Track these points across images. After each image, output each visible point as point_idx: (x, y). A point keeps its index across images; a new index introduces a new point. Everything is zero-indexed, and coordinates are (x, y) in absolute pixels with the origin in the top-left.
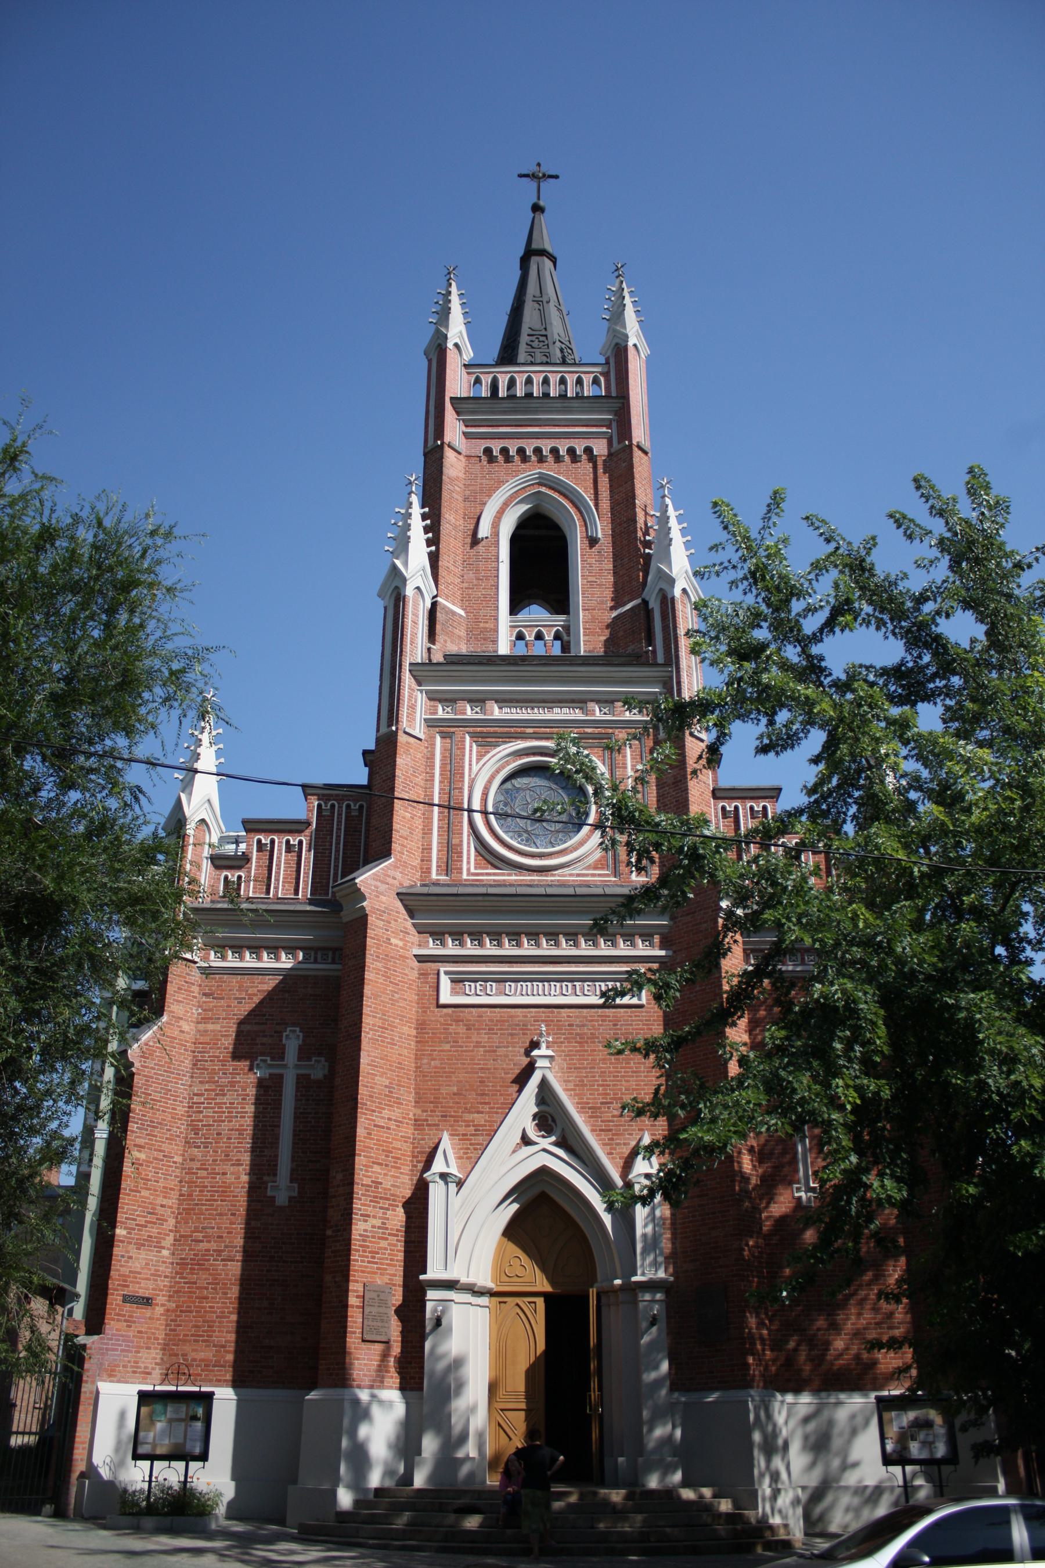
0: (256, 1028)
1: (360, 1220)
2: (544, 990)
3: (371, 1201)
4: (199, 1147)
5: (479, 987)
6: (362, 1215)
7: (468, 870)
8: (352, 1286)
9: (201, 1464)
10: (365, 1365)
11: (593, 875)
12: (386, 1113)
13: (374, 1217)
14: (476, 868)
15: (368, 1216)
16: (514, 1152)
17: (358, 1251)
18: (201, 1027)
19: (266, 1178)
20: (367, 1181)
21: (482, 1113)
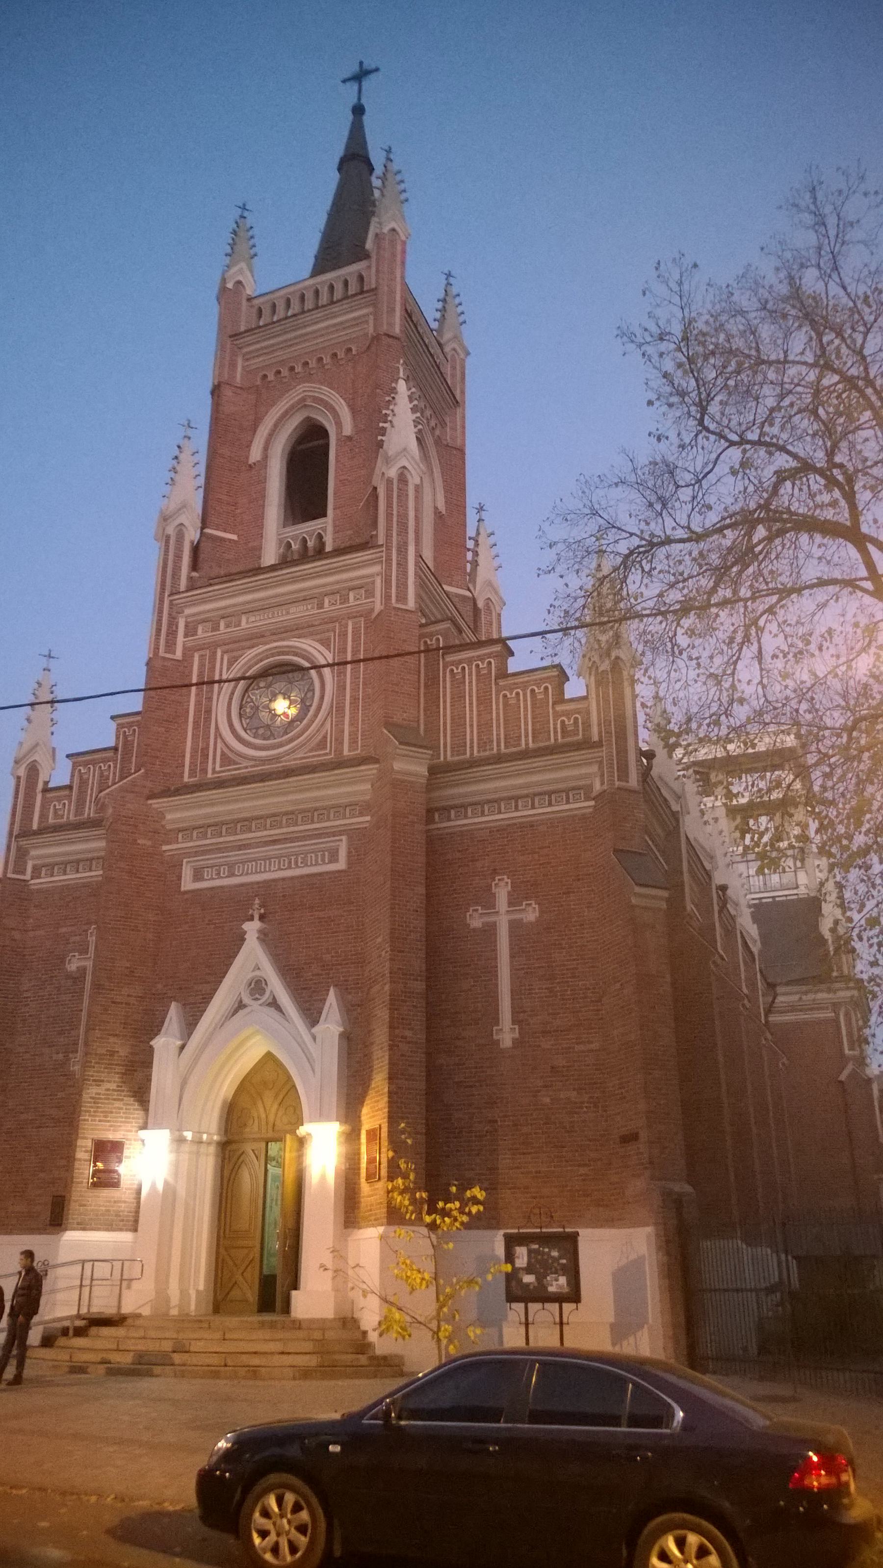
0: (70, 929)
1: (91, 1085)
2: (265, 867)
3: (105, 1068)
4: (25, 1034)
5: (214, 872)
6: (94, 1081)
7: (214, 769)
8: (80, 1142)
9: (574, 1306)
10: (92, 1210)
11: (314, 756)
12: (125, 991)
13: (109, 1082)
14: (221, 767)
15: (103, 1081)
16: (233, 1015)
17: (89, 1111)
18: (31, 934)
19: (71, 1055)
20: (104, 1051)
21: (209, 982)
